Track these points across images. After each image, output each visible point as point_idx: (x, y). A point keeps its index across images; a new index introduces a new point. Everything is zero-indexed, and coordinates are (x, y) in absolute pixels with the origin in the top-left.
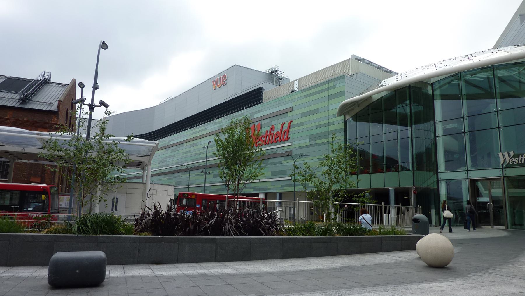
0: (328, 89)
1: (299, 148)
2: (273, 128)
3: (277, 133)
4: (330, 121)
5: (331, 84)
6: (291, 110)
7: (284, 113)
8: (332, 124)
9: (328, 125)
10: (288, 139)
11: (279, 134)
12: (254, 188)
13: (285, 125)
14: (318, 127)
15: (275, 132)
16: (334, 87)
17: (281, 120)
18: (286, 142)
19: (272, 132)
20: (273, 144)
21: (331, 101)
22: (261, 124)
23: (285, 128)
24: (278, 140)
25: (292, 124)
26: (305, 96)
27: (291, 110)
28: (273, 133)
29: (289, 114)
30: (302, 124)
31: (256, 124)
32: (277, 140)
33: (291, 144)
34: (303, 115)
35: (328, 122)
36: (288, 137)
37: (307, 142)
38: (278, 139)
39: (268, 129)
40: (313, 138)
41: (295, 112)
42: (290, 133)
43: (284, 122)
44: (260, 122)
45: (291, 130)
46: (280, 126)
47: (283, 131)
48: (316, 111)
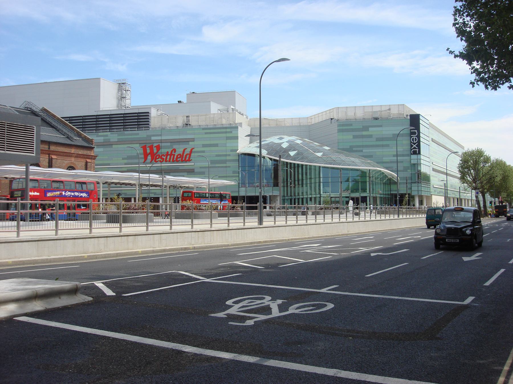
0: (226, 132)
1: (201, 167)
2: (175, 150)
3: (178, 155)
4: (228, 153)
5: (228, 130)
6: (193, 140)
7: (186, 141)
8: (229, 155)
9: (226, 155)
10: (189, 160)
11: (181, 156)
12: (155, 194)
13: (186, 150)
14: (217, 156)
15: (176, 154)
16: (231, 132)
17: (185, 146)
18: (187, 162)
19: (173, 153)
20: (174, 163)
21: (228, 141)
22: (160, 145)
23: (188, 151)
24: (180, 160)
25: (193, 150)
26: (206, 133)
27: (193, 140)
28: (175, 154)
29: (191, 143)
30: (204, 152)
31: (155, 145)
32: (178, 159)
33: (193, 164)
34: (204, 146)
35: (226, 154)
36: (190, 159)
37: (206, 164)
38: (180, 159)
39: (170, 150)
40: (212, 162)
41: (195, 143)
42: (191, 156)
43: (186, 147)
44: (160, 144)
45: (192, 154)
46: (182, 150)
47: (185, 154)
48: (216, 145)
